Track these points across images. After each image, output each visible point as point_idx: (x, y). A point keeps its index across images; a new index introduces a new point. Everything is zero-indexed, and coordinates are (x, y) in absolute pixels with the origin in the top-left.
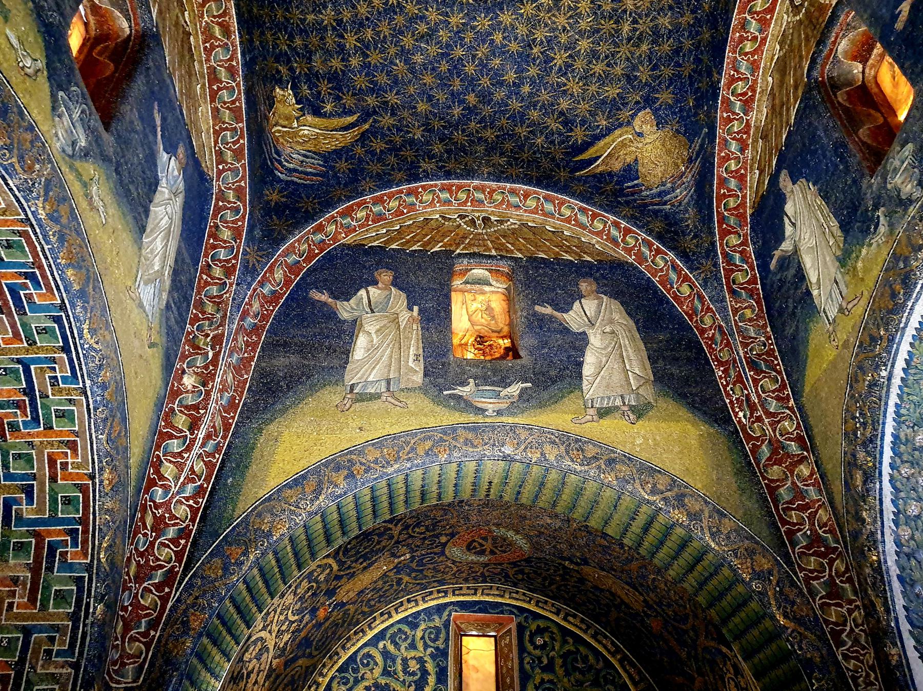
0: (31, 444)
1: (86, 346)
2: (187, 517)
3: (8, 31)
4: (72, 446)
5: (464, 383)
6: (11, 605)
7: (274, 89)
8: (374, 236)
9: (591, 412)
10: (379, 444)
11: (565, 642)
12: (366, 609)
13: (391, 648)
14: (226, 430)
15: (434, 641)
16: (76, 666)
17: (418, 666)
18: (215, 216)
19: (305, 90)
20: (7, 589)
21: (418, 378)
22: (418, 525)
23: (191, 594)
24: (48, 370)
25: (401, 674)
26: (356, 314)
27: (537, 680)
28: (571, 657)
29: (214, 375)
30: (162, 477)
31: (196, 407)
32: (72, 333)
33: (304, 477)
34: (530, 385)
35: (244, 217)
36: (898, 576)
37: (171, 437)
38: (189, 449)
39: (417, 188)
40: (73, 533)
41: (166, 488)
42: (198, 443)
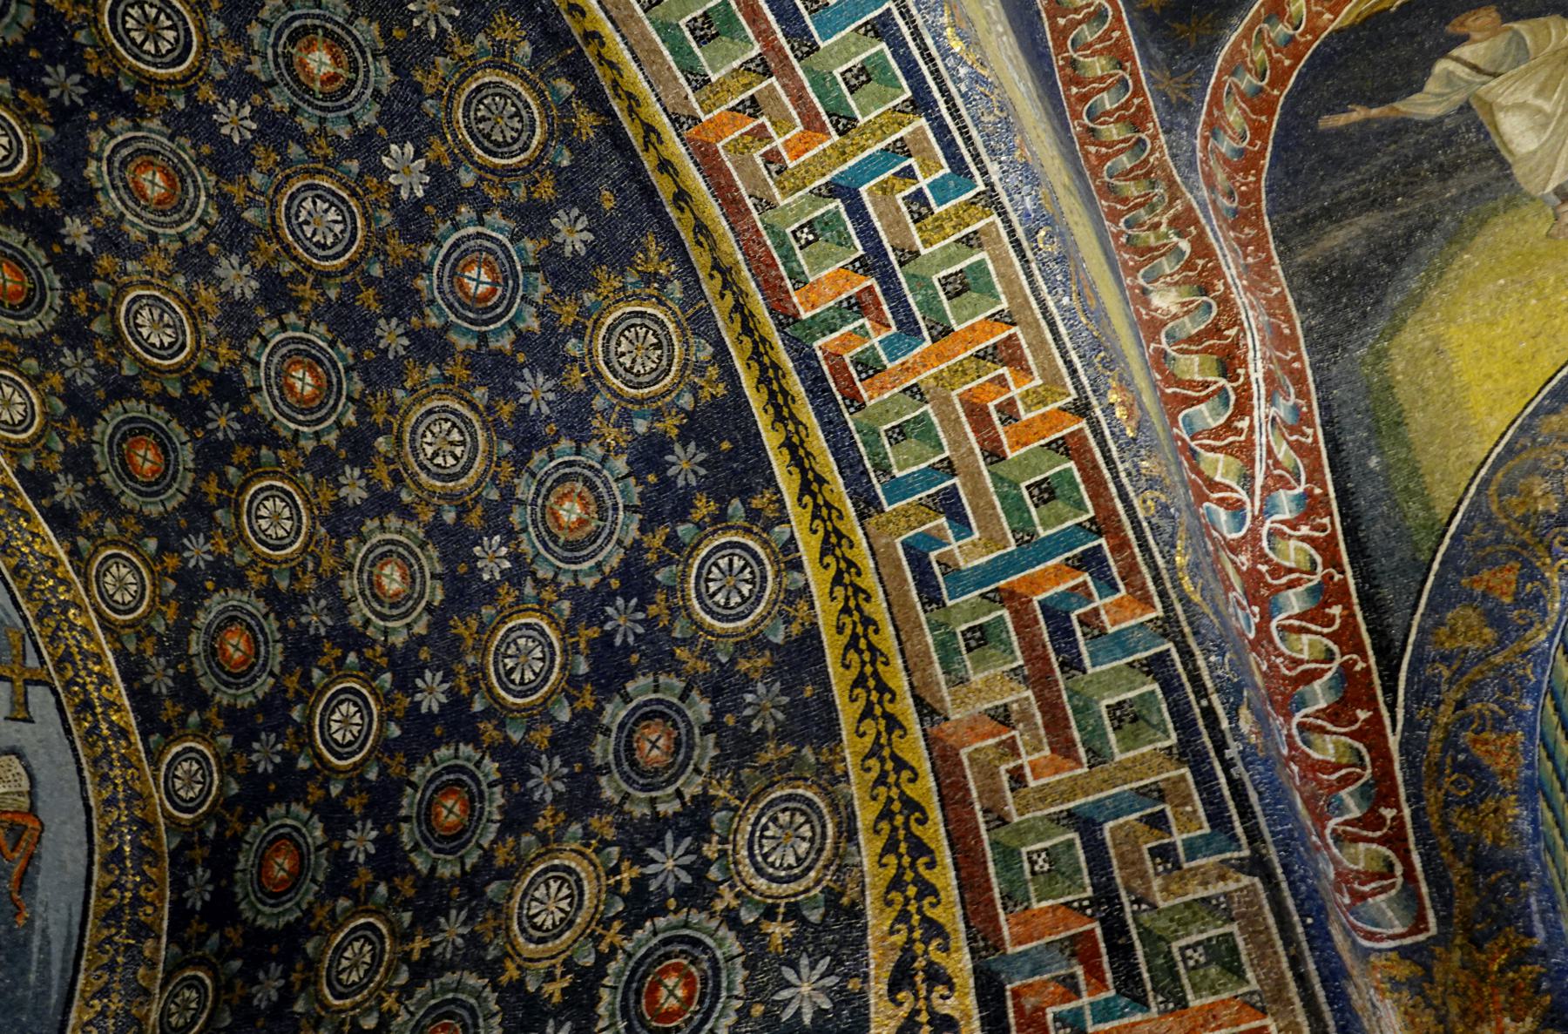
0: (914, 391)
1: (963, 71)
2: (1313, 563)
4: (1007, 354)
6: (1017, 777)
16: (1257, 865)
18: (1060, 47)
20: (991, 741)
23: (1438, 703)
24: (898, 183)
26: (1458, 98)
29: (1218, 267)
30: (1214, 486)
31: (1215, 331)
32: (924, 49)
35: (1119, 19)
37: (1189, 402)
38: (1243, 407)
40: (1091, 561)
41: (1236, 508)
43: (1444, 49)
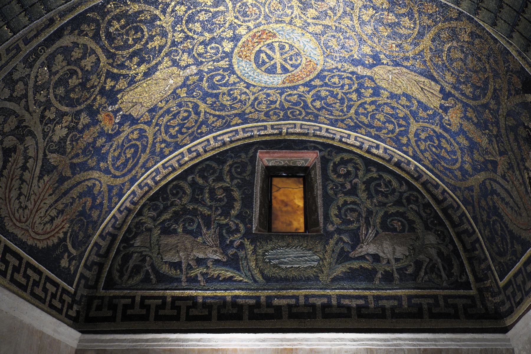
11: (368, 171)
12: (169, 140)
13: (200, 181)
15: (240, 173)
17: (224, 194)
22: (191, 19)
27: (341, 202)
28: (373, 184)
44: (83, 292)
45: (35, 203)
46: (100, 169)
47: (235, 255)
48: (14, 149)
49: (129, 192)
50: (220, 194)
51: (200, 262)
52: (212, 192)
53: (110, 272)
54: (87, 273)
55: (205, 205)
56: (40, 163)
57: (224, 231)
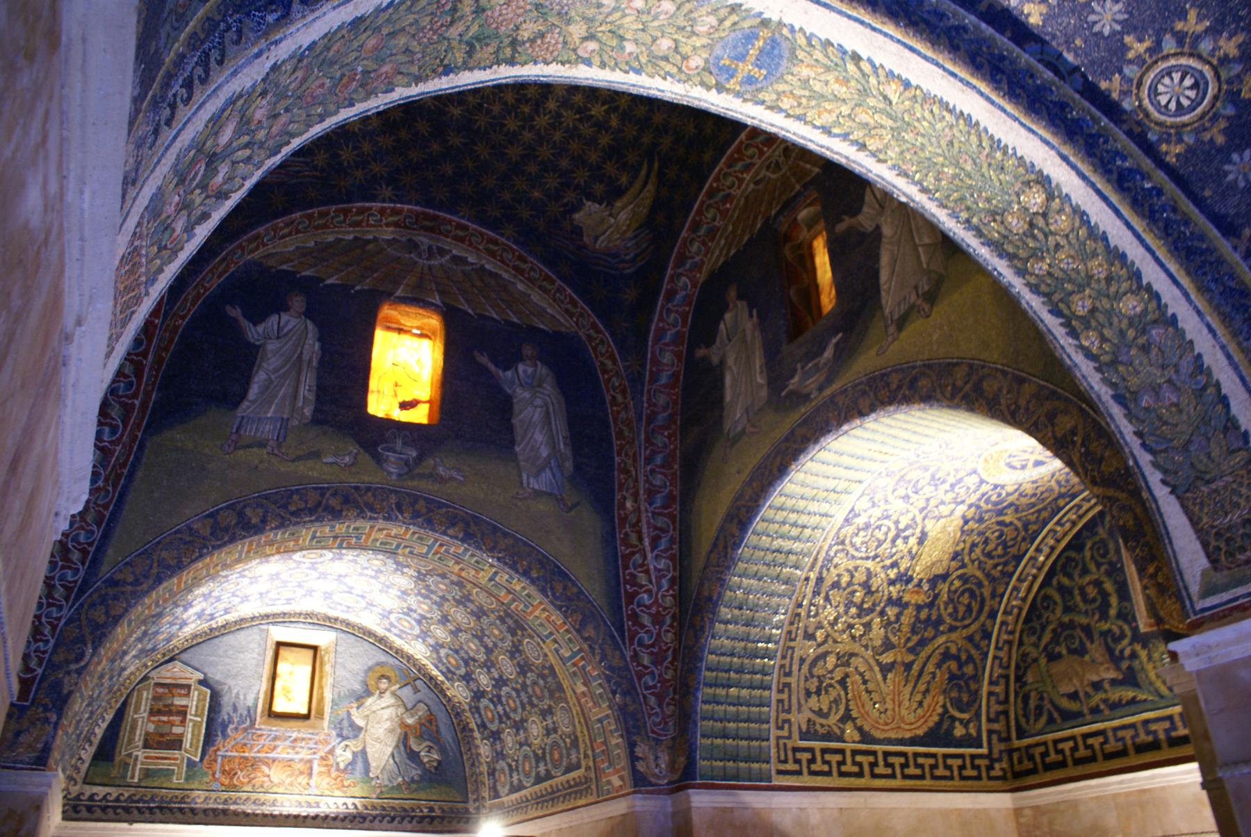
3: (325, 460)
5: (792, 377)
7: (572, 220)
8: (715, 257)
9: (892, 329)
10: (749, 483)
13: (1065, 581)
14: (674, 523)
15: (1104, 556)
19: (599, 188)
21: (764, 393)
25: (1081, 605)
30: (642, 586)
33: (717, 538)
34: (840, 335)
36: (1113, 397)
37: (633, 553)
38: (645, 558)
39: (711, 186)
41: (649, 592)
42: (648, 549)
43: (721, 317)
44: (998, 747)
45: (893, 700)
46: (943, 633)
47: (1130, 668)
48: (847, 675)
49: (997, 627)
50: (1092, 592)
51: (1097, 686)
52: (1082, 590)
53: (1017, 719)
54: (996, 726)
55: (1079, 612)
56: (877, 669)
57: (1109, 640)
